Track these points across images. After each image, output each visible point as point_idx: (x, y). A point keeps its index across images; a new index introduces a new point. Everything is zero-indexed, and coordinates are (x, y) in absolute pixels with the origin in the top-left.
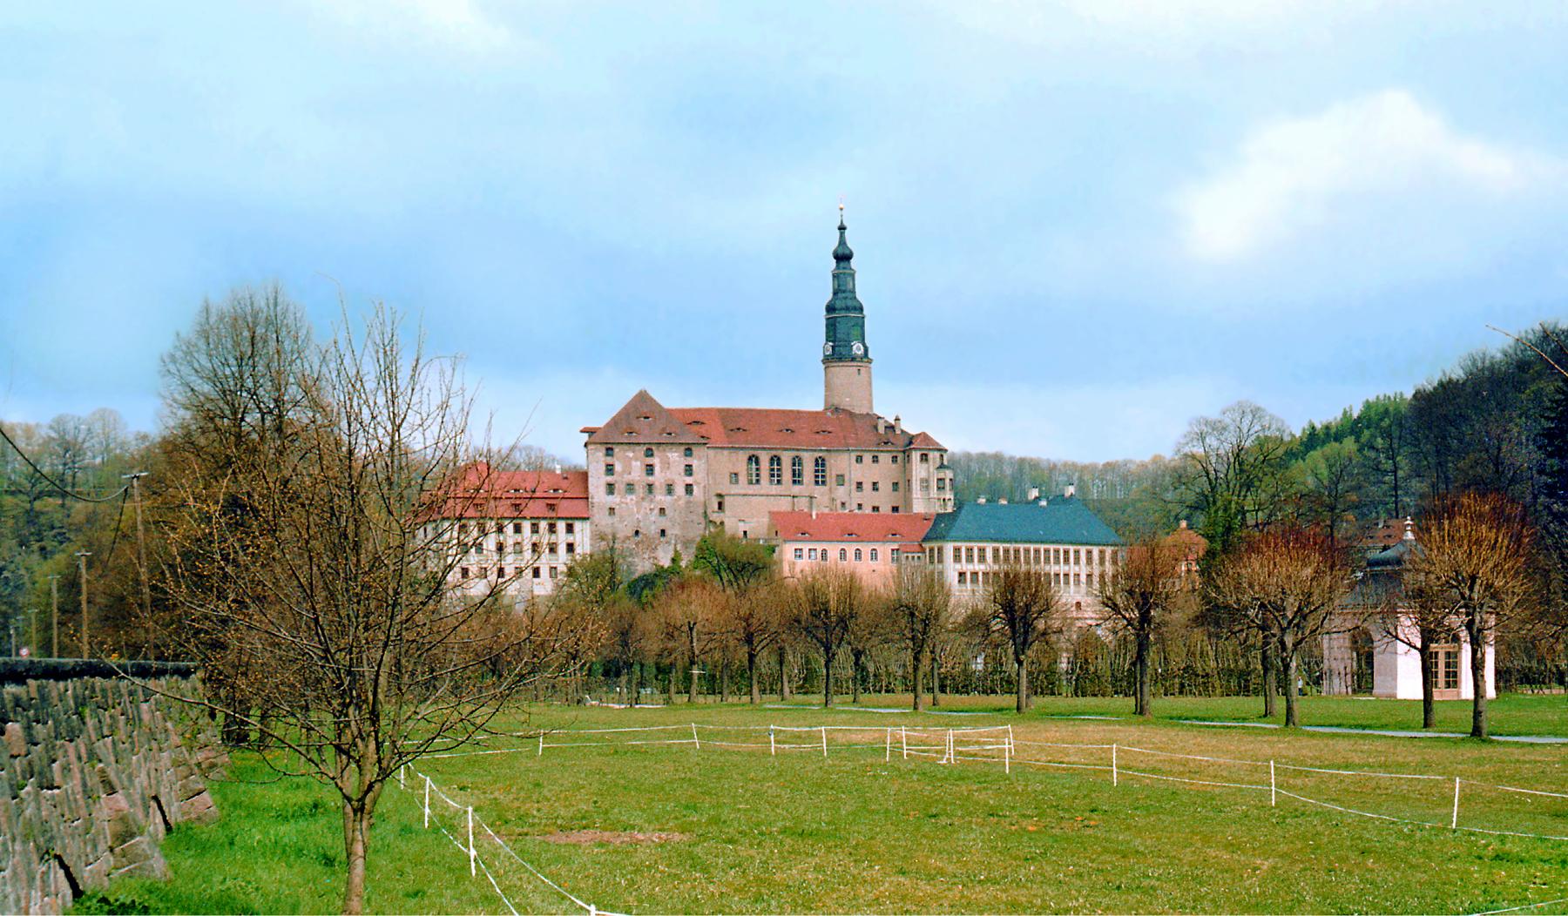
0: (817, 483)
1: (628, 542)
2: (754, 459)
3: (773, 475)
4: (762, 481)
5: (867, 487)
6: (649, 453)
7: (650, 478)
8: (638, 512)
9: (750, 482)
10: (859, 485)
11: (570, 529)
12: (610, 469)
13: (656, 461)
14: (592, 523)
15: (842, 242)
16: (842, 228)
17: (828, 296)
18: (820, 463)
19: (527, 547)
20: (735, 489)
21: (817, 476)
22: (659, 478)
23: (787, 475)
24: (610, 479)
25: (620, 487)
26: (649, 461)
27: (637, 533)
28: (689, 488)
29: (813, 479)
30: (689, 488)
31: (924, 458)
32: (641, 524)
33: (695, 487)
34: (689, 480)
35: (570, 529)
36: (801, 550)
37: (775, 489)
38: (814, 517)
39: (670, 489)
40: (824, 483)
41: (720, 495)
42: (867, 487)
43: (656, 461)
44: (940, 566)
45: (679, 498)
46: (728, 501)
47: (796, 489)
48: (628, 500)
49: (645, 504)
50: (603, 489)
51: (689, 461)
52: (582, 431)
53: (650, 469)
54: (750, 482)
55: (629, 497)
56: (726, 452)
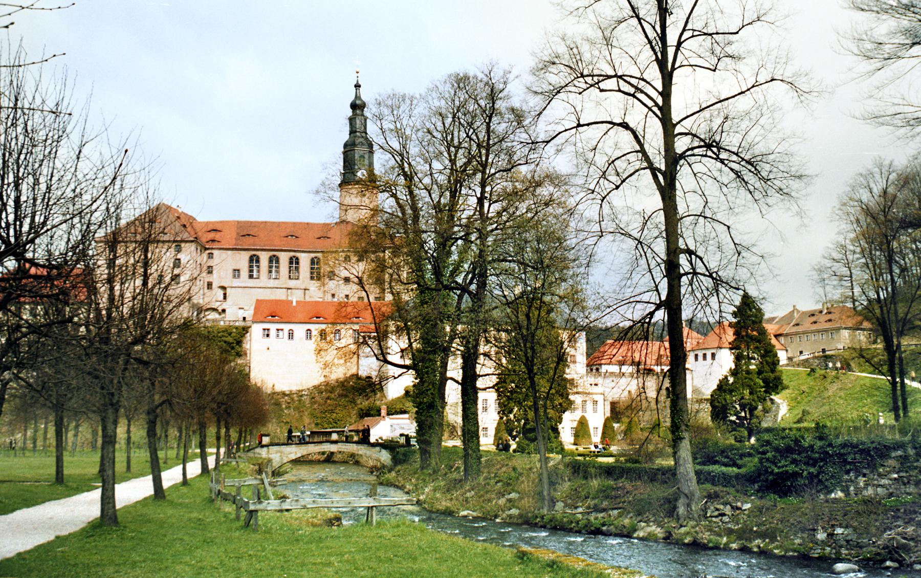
0: (312, 278)
2: (254, 260)
4: (261, 277)
9: (251, 277)
15: (357, 97)
16: (357, 86)
17: (346, 137)
20: (236, 282)
21: (312, 273)
29: (308, 275)
36: (268, 330)
37: (272, 283)
38: (294, 304)
41: (224, 288)
46: (228, 291)
54: (251, 277)
56: (229, 252)
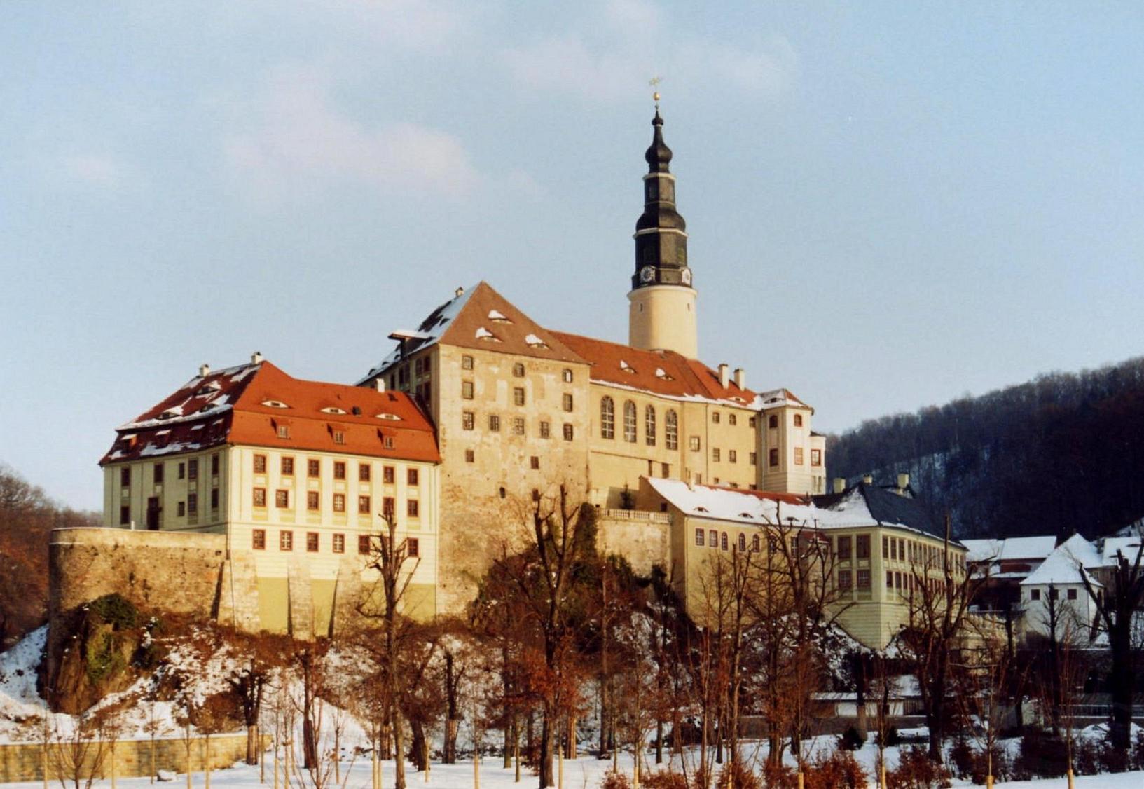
1: (489, 504)
3: (627, 429)
5: (725, 455)
6: (520, 372)
7: (521, 409)
8: (505, 458)
10: (717, 452)
11: (413, 478)
12: (469, 392)
13: (527, 383)
14: (442, 472)
16: (657, 122)
18: (672, 417)
19: (353, 504)
22: (531, 412)
23: (642, 435)
24: (468, 404)
25: (482, 421)
26: (520, 382)
27: (503, 491)
28: (568, 432)
30: (568, 432)
31: (799, 420)
32: (508, 480)
33: (575, 430)
34: (568, 418)
35: (413, 478)
37: (629, 449)
39: (545, 432)
40: (676, 447)
42: (725, 455)
43: (527, 383)
44: (864, 563)
45: (555, 445)
47: (650, 452)
48: (491, 441)
49: (513, 448)
50: (458, 421)
51: (570, 389)
52: (392, 337)
53: (520, 396)
55: (494, 435)
